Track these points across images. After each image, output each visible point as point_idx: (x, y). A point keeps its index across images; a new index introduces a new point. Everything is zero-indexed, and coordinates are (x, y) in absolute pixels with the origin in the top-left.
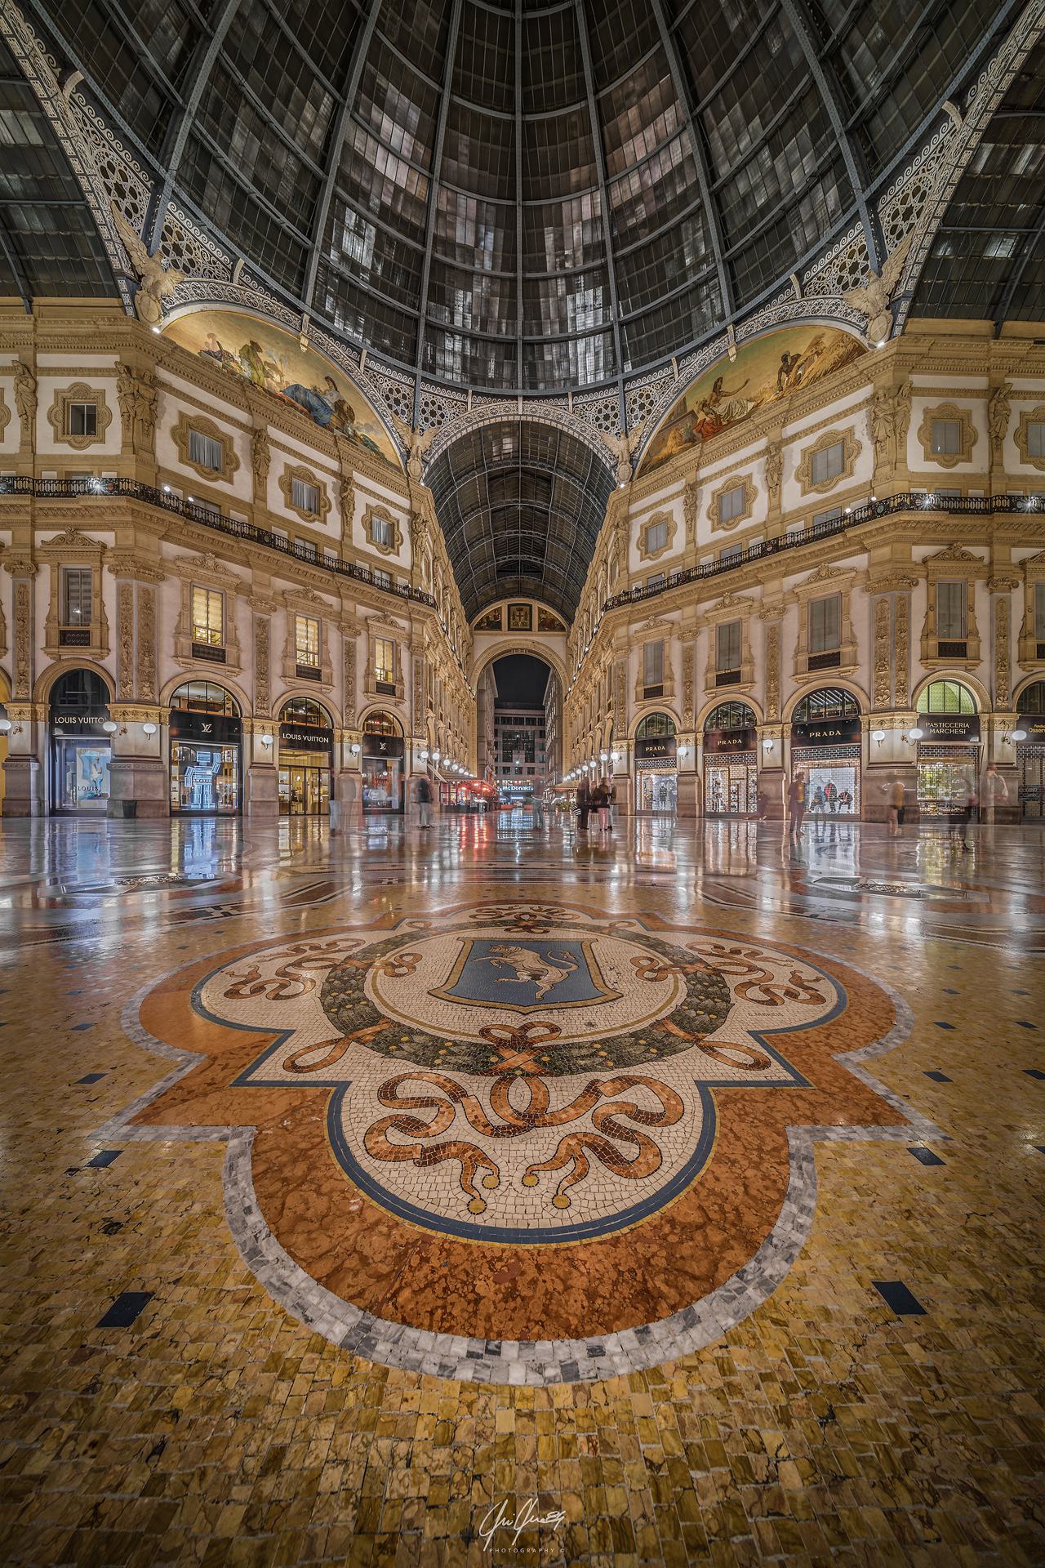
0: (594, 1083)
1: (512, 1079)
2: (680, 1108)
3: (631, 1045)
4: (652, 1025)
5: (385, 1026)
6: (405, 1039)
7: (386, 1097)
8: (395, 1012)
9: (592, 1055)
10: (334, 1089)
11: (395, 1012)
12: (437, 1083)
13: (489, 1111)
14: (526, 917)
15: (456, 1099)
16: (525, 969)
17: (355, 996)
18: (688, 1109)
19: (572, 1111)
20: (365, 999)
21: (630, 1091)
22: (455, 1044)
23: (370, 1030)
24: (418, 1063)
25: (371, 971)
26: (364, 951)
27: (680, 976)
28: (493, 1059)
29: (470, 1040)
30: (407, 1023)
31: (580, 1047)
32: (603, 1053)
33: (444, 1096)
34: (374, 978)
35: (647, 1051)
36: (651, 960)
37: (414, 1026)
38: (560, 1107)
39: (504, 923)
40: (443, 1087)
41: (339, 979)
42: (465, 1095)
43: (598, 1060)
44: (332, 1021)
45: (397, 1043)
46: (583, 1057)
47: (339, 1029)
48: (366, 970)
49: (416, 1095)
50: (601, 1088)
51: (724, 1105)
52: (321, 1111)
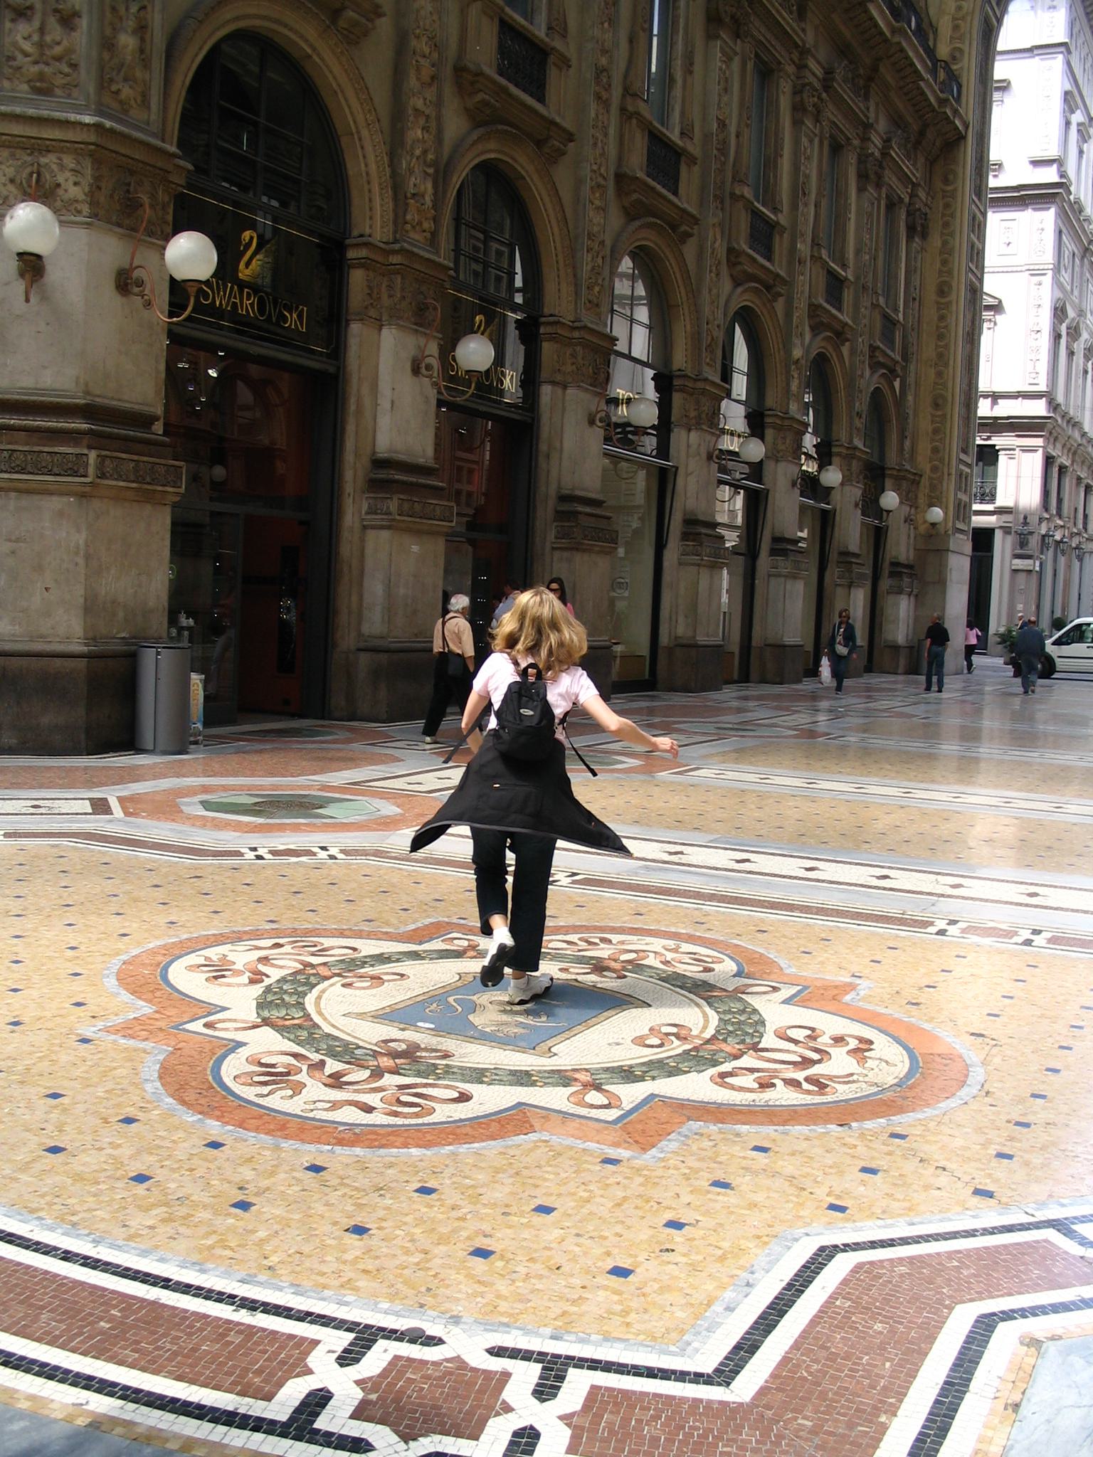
20: (718, 1012)
26: (715, 1063)
34: (705, 1027)
41: (747, 1034)
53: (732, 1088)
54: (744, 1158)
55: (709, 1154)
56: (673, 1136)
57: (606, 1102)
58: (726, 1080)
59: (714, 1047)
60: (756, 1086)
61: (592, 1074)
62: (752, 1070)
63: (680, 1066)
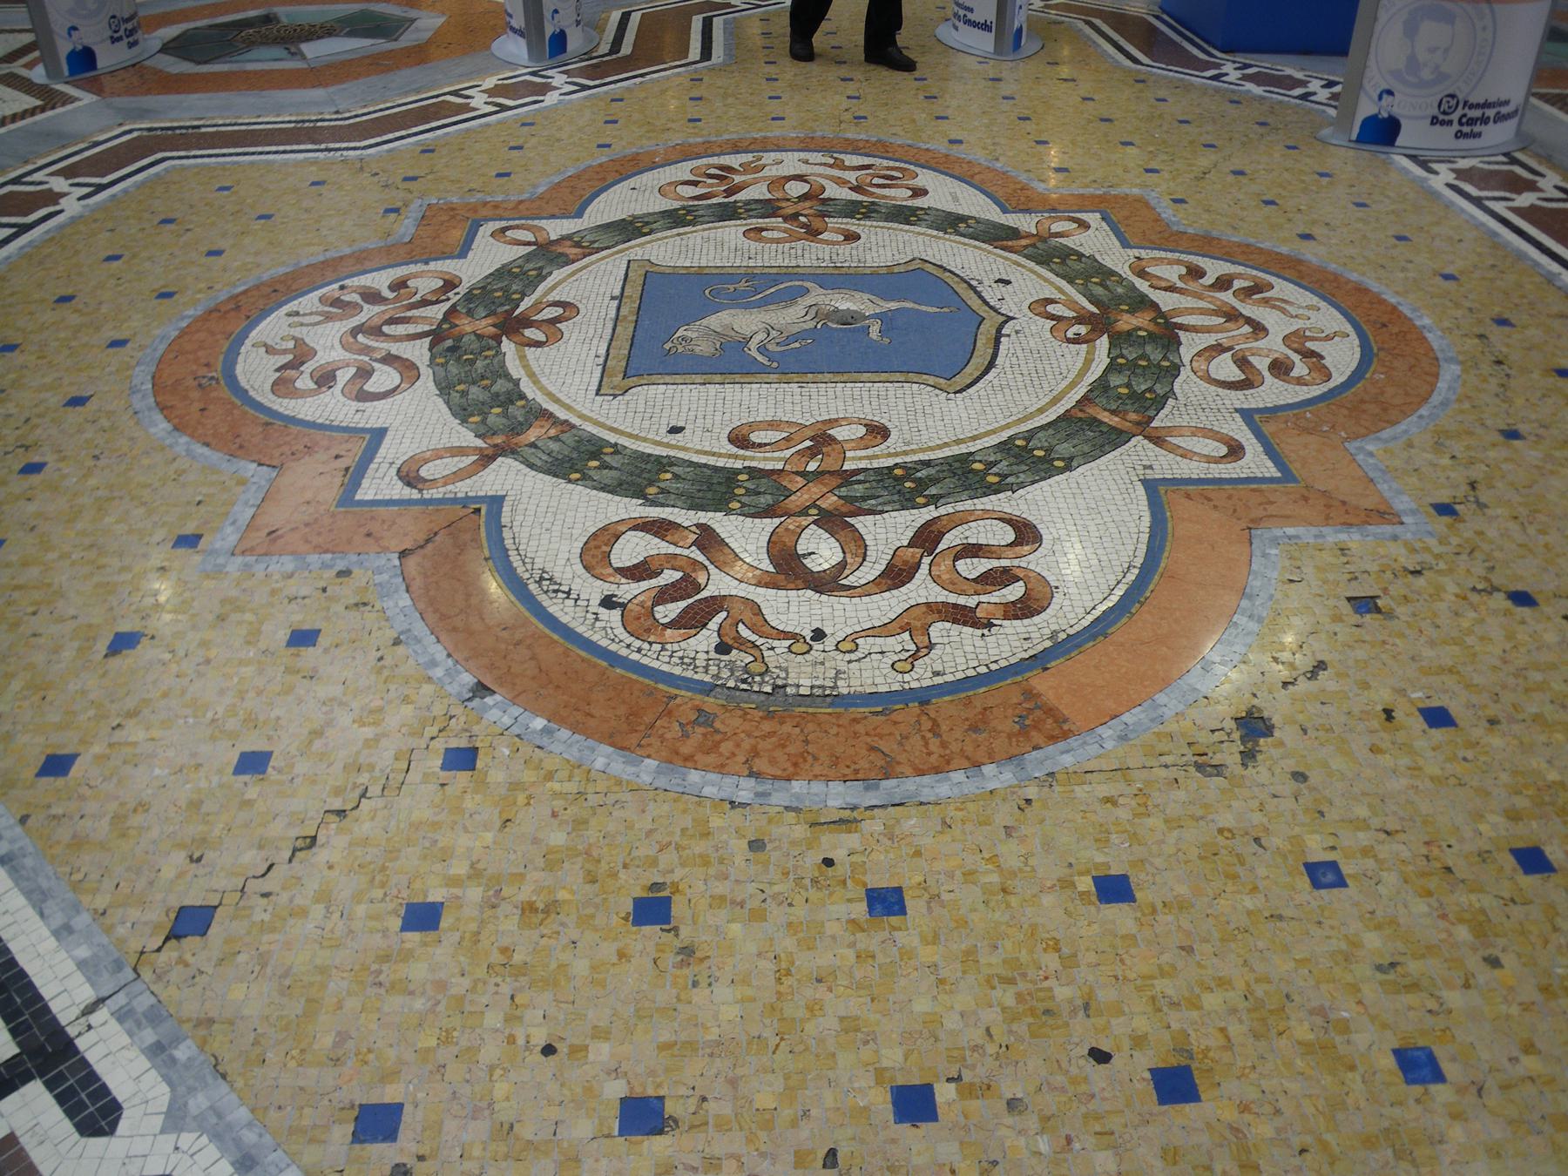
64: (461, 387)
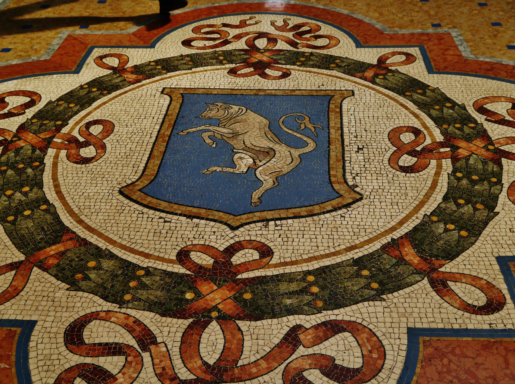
0: (297, 328)
1: (206, 324)
2: (380, 362)
3: (351, 278)
4: (384, 248)
5: (70, 244)
6: (92, 264)
7: (74, 343)
8: (80, 222)
9: (304, 291)
10: (19, 330)
11: (80, 222)
12: (125, 326)
13: (178, 362)
14: (261, 43)
15: (145, 348)
16: (247, 149)
17: (32, 195)
18: (388, 363)
19: (264, 364)
20: (46, 201)
21: (332, 340)
22: (148, 272)
23: (53, 250)
24: (105, 298)
25: (51, 152)
26: (39, 115)
27: (447, 165)
28: (189, 296)
29: (165, 267)
30: (93, 239)
31: (290, 278)
32: (315, 289)
33: (133, 342)
34: (55, 165)
35: (368, 286)
36: (416, 132)
37: (102, 244)
38: (253, 359)
39: (229, 57)
40: (131, 331)
42: (154, 342)
43: (307, 298)
44: (9, 234)
45: (83, 269)
46: (291, 294)
47: (19, 247)
48: (44, 150)
49: (104, 340)
50: (302, 337)
51: (429, 359)
52: (9, 357)
53: (24, 93)
54: (15, 43)
55: (34, 42)
56: (57, 47)
57: (104, 60)
58: (28, 99)
59: (42, 136)
60: (7, 99)
61: (125, 80)
62: (10, 115)
63: (65, 105)
64: (9, 192)
